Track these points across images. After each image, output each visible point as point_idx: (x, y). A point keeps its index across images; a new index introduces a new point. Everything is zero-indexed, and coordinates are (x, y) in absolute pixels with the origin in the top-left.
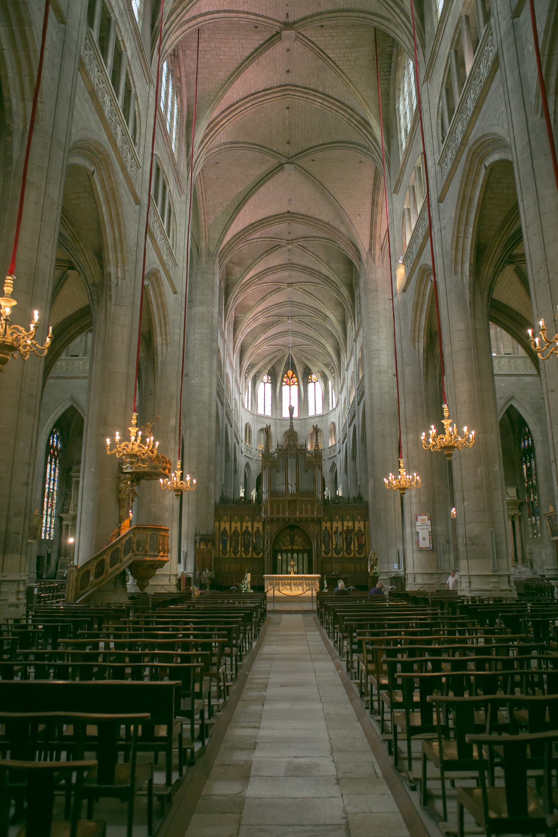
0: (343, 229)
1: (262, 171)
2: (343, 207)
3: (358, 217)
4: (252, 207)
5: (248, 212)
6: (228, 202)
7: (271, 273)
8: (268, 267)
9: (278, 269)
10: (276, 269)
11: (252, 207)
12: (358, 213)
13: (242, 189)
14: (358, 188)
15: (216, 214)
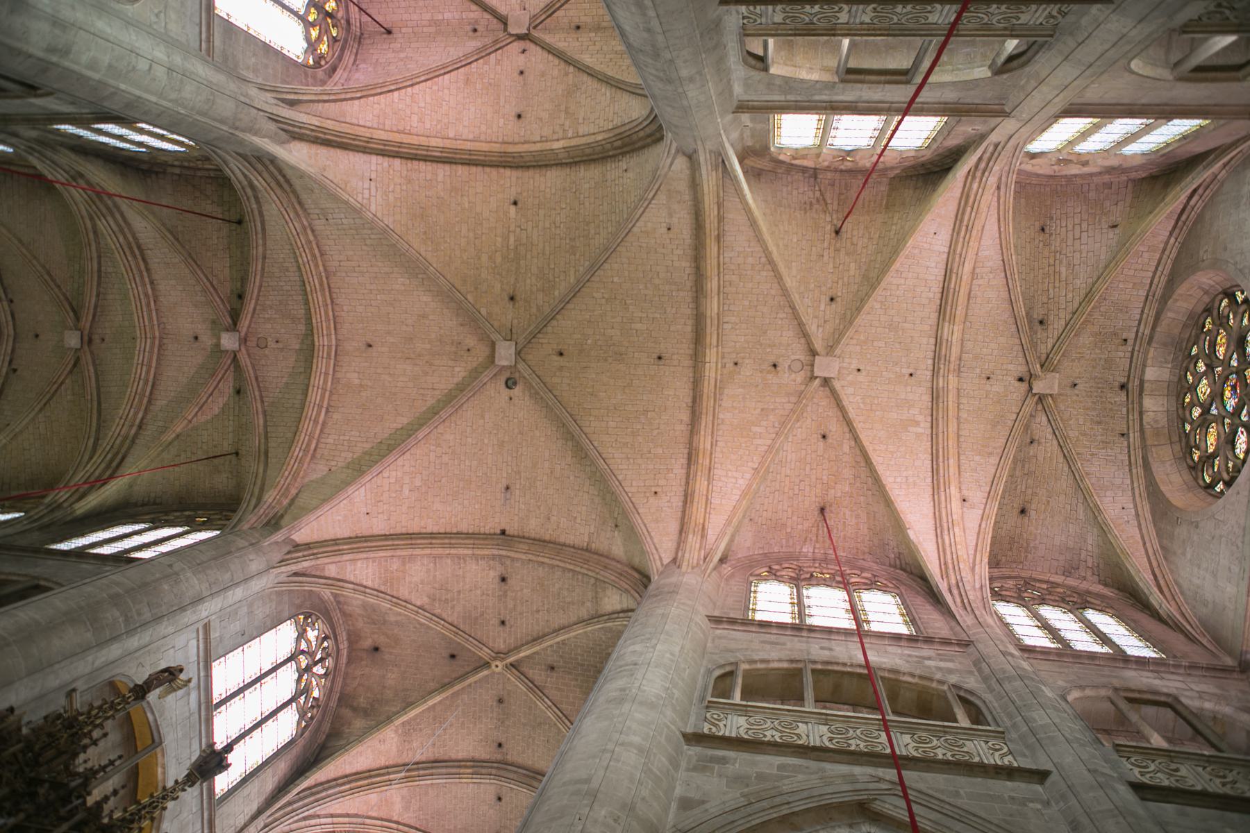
0: (618, 550)
1: (456, 380)
2: (620, 478)
3: (652, 500)
4: (418, 483)
5: (406, 492)
6: (367, 446)
7: (444, 770)
8: (440, 753)
9: (466, 767)
10: (459, 767)
11: (418, 483)
12: (654, 489)
13: (405, 421)
14: (655, 432)
15: (334, 463)
